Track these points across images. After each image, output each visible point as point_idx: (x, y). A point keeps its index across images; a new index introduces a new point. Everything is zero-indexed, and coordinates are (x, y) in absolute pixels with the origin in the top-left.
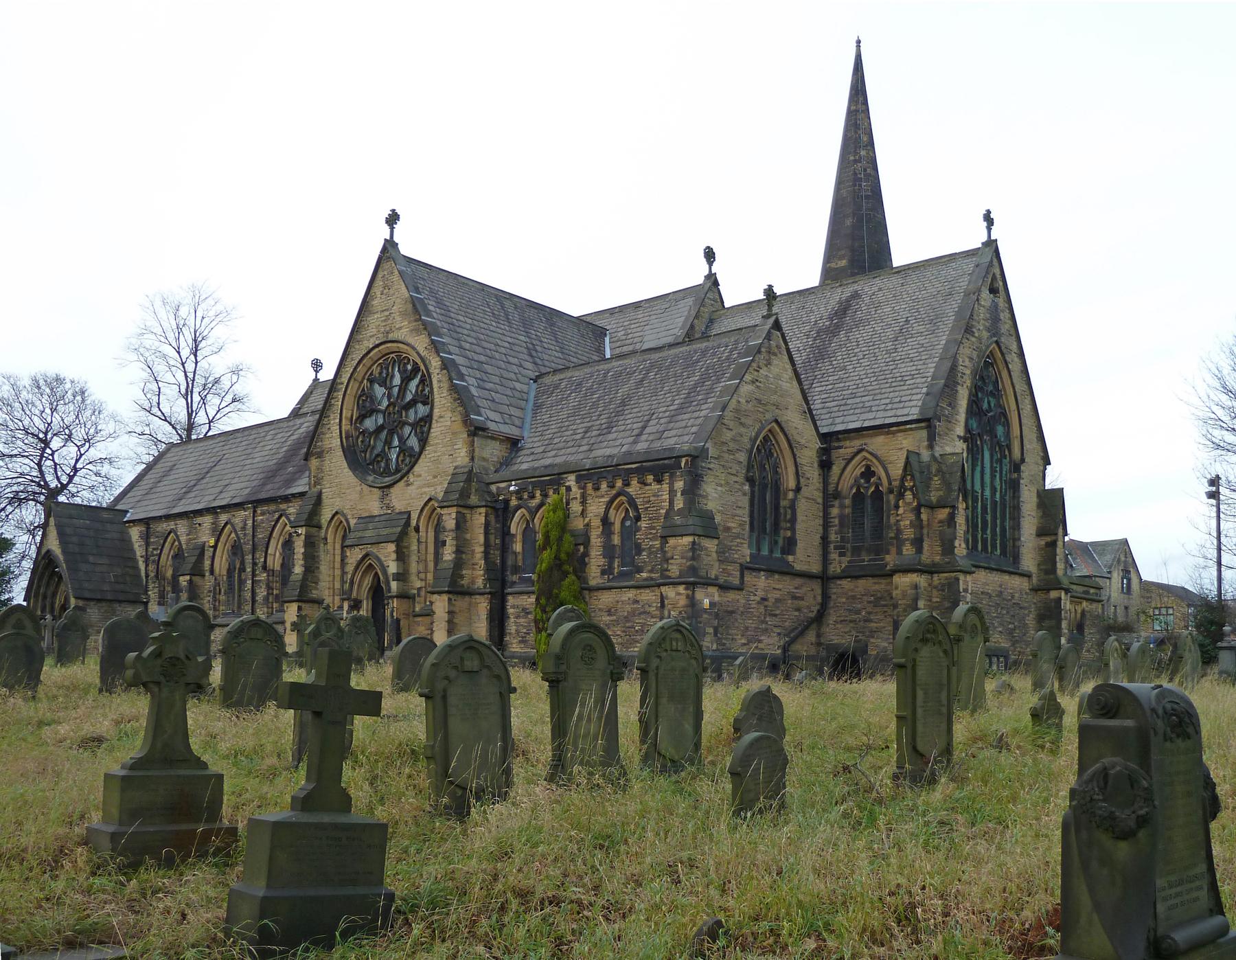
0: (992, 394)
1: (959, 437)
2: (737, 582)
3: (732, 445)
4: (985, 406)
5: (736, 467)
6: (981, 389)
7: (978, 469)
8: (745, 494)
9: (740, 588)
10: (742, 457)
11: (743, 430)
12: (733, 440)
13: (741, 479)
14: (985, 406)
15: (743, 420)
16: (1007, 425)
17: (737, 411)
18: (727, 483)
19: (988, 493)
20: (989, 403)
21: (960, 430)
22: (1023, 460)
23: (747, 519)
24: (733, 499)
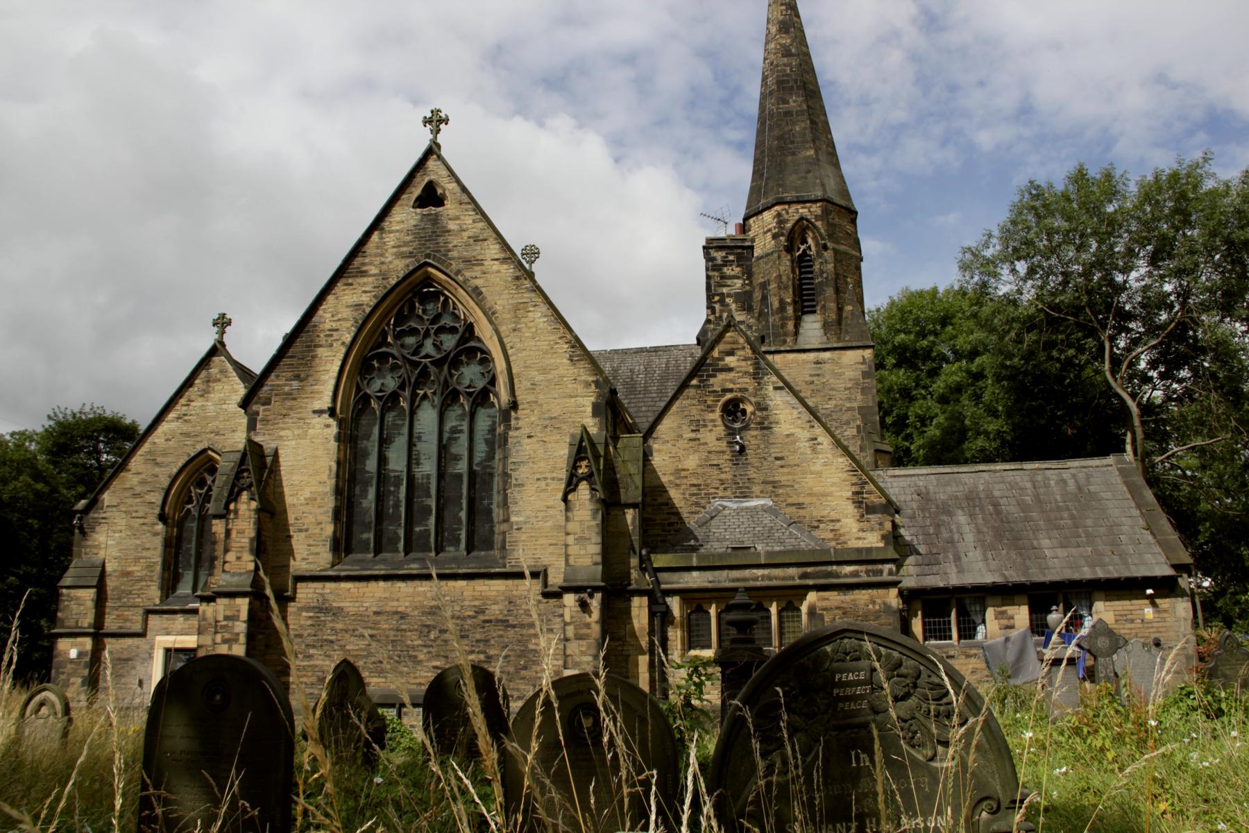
0: (442, 330)
1: (319, 412)
2: (137, 627)
3: (139, 489)
4: (429, 347)
5: (142, 510)
6: (414, 332)
7: (401, 442)
8: (156, 534)
9: (142, 635)
10: (157, 498)
11: (157, 470)
12: (143, 482)
13: (152, 518)
14: (429, 347)
15: (159, 460)
16: (486, 360)
17: (150, 452)
18: (131, 527)
19: (428, 467)
20: (437, 347)
21: (325, 402)
22: (514, 405)
23: (159, 560)
24: (138, 542)
